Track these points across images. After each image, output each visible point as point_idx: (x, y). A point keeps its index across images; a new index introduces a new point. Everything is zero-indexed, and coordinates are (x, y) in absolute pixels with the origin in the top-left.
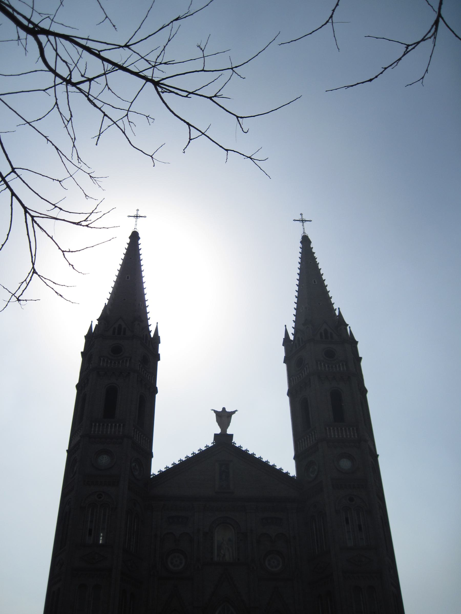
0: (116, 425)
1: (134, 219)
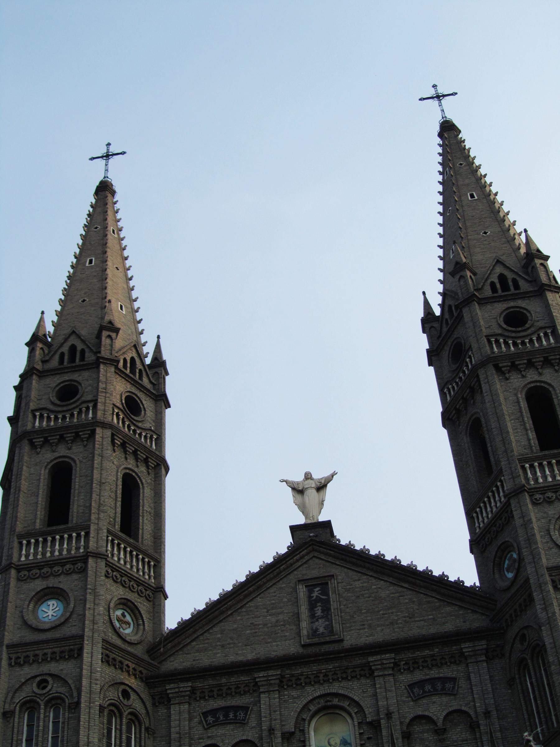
0: (70, 537)
1: (102, 162)
